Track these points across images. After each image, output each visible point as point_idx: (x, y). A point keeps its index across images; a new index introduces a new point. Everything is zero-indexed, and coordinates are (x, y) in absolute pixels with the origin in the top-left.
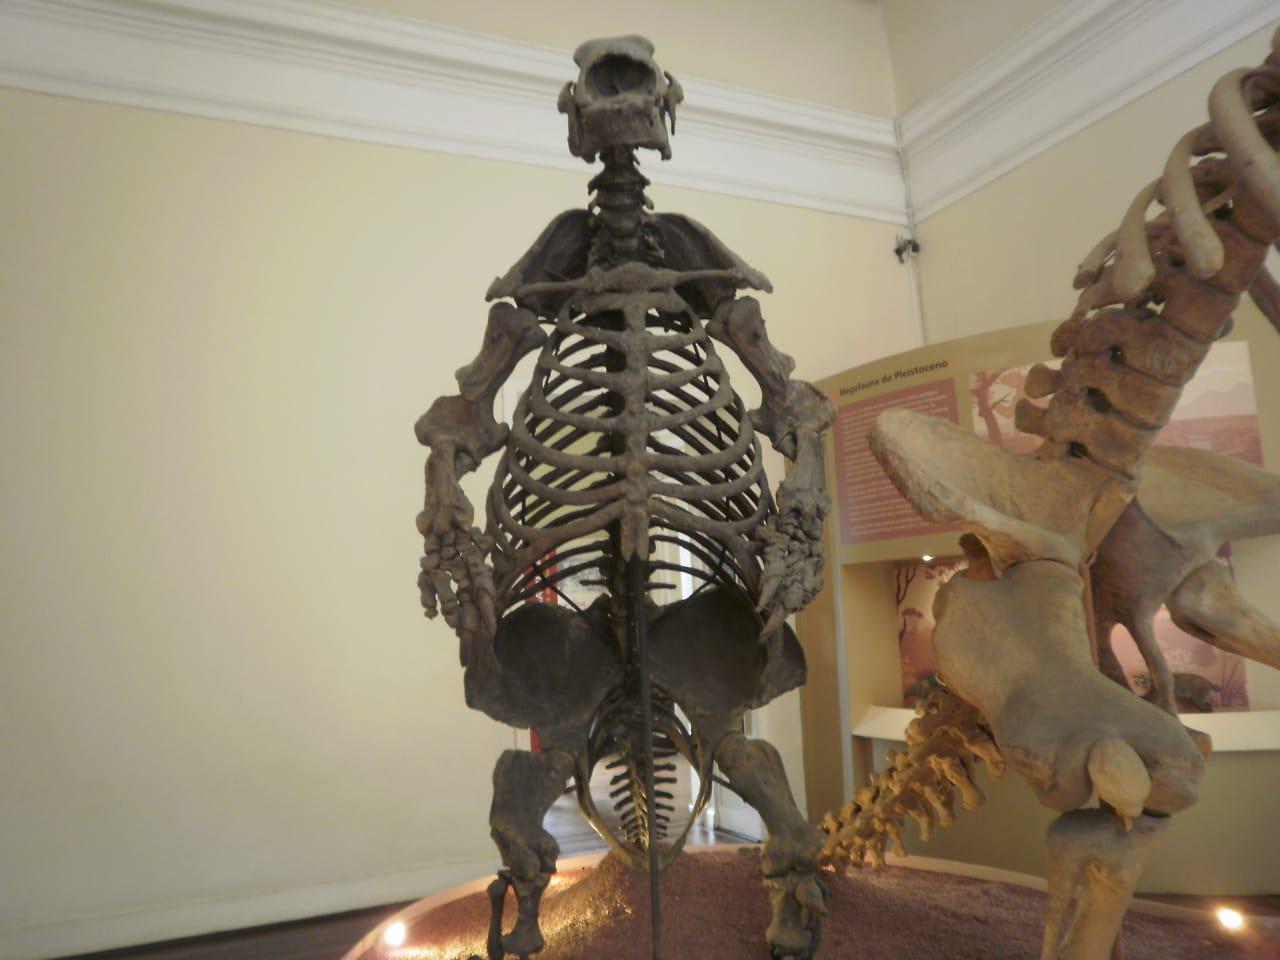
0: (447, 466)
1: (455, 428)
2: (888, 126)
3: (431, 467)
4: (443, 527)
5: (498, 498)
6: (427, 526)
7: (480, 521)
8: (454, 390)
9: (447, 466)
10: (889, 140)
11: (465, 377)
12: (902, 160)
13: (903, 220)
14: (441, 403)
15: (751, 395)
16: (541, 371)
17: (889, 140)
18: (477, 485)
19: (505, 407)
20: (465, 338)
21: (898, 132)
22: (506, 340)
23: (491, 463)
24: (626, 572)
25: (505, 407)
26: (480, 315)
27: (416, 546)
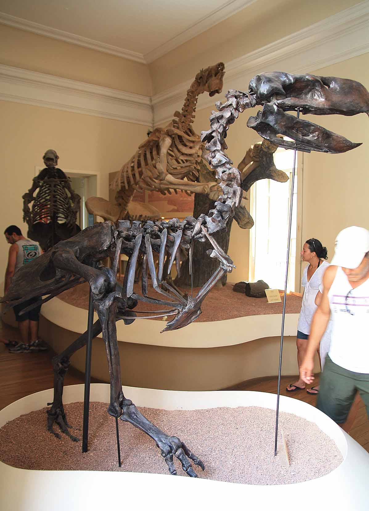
0: (27, 203)
1: (28, 197)
2: (148, 99)
3: (24, 202)
4: (26, 210)
5: (34, 206)
6: (24, 211)
7: (31, 210)
8: (28, 192)
9: (27, 203)
10: (148, 103)
11: (29, 190)
12: (152, 108)
13: (151, 125)
14: (26, 194)
15: (69, 195)
16: (40, 191)
17: (148, 103)
18: (30, 205)
19: (35, 195)
20: (30, 186)
21: (151, 100)
22: (36, 184)
23: (33, 202)
24: (54, 218)
25: (35, 195)
26: (32, 183)
27: (22, 213)
